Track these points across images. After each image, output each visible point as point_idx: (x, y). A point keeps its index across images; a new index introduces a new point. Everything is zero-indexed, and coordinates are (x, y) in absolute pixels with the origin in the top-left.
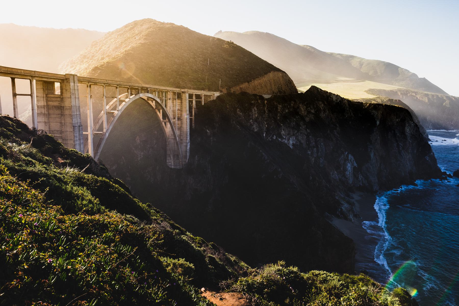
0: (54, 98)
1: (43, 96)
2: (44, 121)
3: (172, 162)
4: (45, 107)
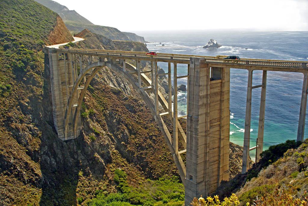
0: (215, 84)
1: (206, 84)
2: (205, 112)
3: (66, 134)
4: (209, 96)
